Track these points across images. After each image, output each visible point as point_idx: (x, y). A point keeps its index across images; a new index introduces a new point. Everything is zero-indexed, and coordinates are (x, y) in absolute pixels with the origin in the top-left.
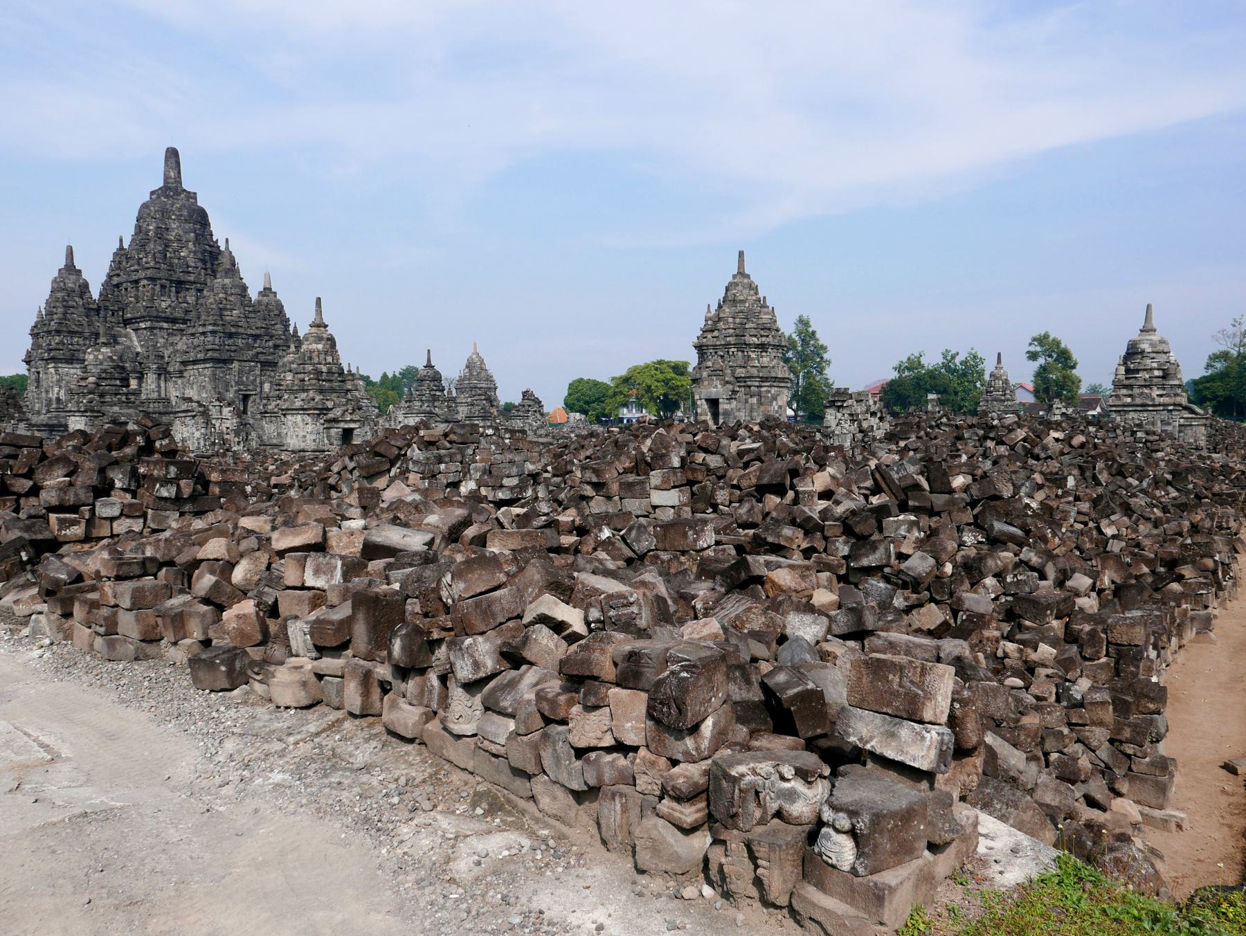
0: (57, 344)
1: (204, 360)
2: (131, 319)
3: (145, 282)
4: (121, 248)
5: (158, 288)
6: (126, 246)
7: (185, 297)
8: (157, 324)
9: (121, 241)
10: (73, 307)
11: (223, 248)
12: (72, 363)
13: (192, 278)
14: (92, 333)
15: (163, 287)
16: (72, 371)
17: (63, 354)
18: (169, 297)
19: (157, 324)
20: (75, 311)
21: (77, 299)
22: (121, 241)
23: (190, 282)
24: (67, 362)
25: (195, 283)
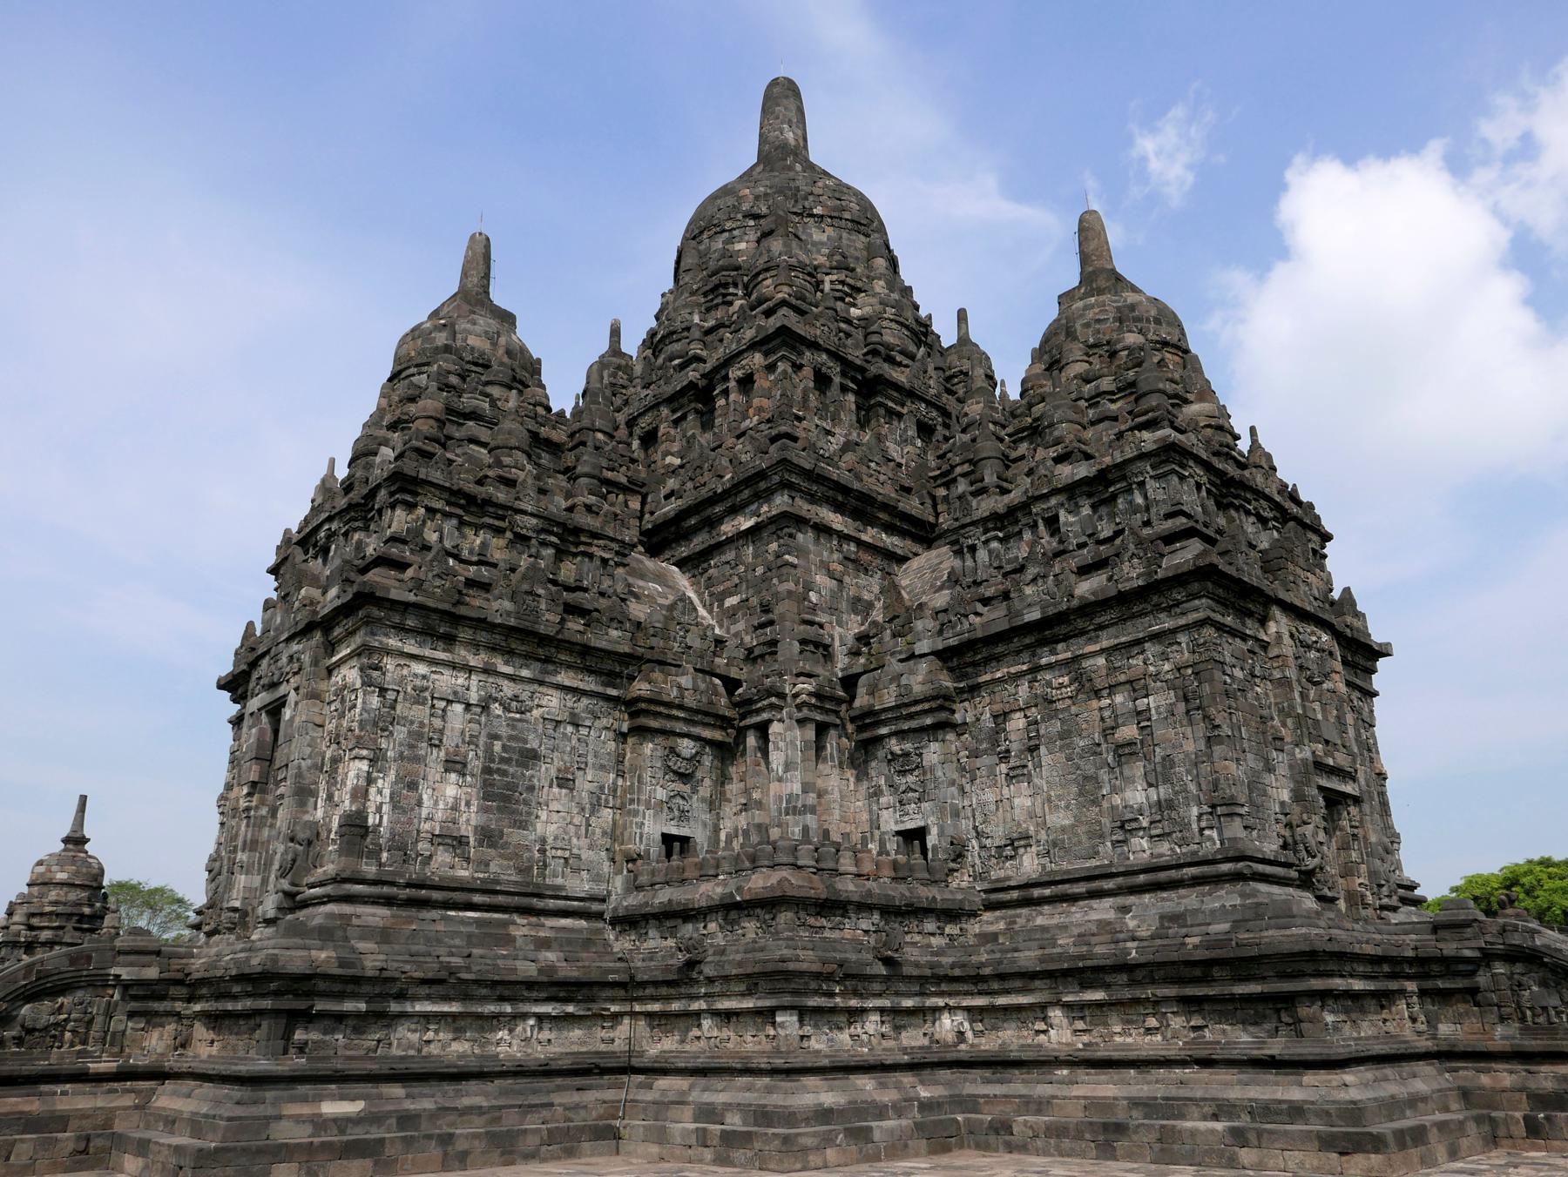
0: (394, 539)
1: (1141, 594)
2: (682, 515)
3: (758, 359)
4: (615, 349)
5: (806, 378)
6: (631, 345)
7: (879, 438)
8: (803, 507)
9: (615, 333)
10: (474, 415)
11: (948, 338)
12: (449, 640)
13: (900, 376)
14: (549, 523)
15: (822, 381)
16: (447, 681)
17: (418, 585)
18: (835, 419)
19: (803, 507)
20: (484, 434)
21: (496, 391)
22: (615, 333)
23: (896, 387)
24: (427, 633)
25: (912, 394)
